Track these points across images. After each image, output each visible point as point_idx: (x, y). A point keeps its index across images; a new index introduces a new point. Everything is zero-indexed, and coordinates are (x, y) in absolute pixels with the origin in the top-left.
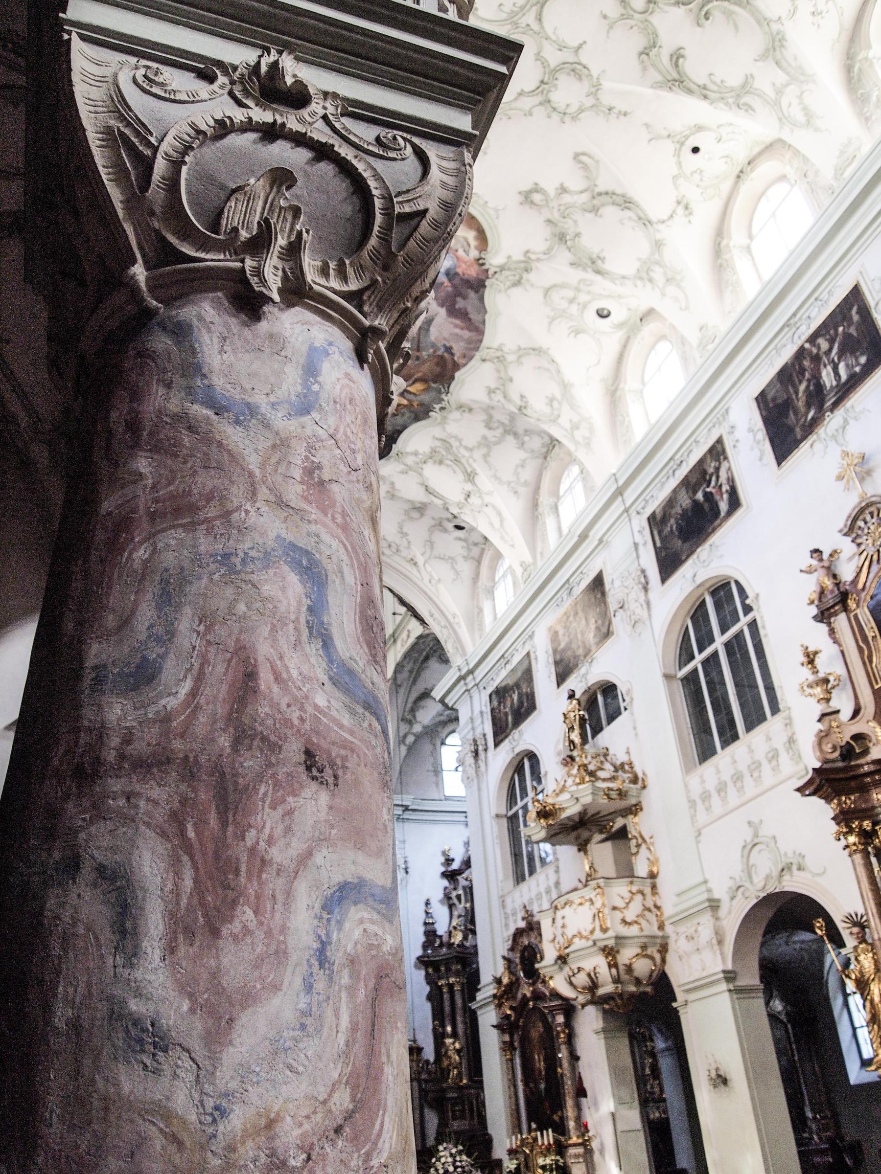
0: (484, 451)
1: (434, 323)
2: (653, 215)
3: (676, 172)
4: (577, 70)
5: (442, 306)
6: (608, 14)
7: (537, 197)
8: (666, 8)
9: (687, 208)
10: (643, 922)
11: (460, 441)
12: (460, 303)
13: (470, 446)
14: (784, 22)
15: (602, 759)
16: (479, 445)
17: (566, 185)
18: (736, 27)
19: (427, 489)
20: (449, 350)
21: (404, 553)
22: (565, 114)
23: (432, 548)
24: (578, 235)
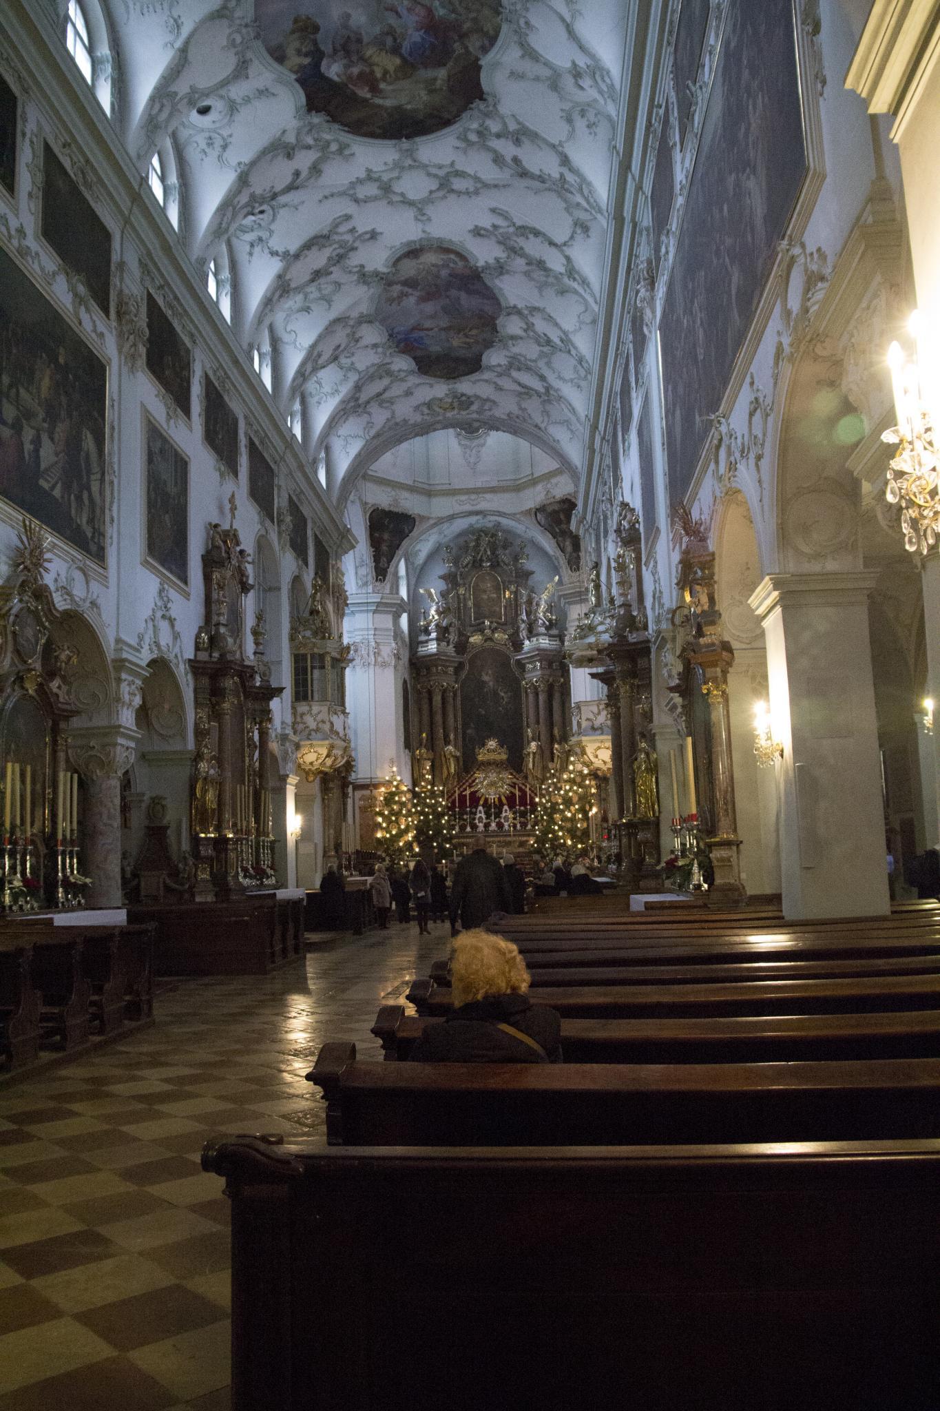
2: (559, 240)
3: (565, 205)
7: (482, 232)
16: (539, 355)
19: (520, 384)
23: (548, 416)
24: (522, 248)
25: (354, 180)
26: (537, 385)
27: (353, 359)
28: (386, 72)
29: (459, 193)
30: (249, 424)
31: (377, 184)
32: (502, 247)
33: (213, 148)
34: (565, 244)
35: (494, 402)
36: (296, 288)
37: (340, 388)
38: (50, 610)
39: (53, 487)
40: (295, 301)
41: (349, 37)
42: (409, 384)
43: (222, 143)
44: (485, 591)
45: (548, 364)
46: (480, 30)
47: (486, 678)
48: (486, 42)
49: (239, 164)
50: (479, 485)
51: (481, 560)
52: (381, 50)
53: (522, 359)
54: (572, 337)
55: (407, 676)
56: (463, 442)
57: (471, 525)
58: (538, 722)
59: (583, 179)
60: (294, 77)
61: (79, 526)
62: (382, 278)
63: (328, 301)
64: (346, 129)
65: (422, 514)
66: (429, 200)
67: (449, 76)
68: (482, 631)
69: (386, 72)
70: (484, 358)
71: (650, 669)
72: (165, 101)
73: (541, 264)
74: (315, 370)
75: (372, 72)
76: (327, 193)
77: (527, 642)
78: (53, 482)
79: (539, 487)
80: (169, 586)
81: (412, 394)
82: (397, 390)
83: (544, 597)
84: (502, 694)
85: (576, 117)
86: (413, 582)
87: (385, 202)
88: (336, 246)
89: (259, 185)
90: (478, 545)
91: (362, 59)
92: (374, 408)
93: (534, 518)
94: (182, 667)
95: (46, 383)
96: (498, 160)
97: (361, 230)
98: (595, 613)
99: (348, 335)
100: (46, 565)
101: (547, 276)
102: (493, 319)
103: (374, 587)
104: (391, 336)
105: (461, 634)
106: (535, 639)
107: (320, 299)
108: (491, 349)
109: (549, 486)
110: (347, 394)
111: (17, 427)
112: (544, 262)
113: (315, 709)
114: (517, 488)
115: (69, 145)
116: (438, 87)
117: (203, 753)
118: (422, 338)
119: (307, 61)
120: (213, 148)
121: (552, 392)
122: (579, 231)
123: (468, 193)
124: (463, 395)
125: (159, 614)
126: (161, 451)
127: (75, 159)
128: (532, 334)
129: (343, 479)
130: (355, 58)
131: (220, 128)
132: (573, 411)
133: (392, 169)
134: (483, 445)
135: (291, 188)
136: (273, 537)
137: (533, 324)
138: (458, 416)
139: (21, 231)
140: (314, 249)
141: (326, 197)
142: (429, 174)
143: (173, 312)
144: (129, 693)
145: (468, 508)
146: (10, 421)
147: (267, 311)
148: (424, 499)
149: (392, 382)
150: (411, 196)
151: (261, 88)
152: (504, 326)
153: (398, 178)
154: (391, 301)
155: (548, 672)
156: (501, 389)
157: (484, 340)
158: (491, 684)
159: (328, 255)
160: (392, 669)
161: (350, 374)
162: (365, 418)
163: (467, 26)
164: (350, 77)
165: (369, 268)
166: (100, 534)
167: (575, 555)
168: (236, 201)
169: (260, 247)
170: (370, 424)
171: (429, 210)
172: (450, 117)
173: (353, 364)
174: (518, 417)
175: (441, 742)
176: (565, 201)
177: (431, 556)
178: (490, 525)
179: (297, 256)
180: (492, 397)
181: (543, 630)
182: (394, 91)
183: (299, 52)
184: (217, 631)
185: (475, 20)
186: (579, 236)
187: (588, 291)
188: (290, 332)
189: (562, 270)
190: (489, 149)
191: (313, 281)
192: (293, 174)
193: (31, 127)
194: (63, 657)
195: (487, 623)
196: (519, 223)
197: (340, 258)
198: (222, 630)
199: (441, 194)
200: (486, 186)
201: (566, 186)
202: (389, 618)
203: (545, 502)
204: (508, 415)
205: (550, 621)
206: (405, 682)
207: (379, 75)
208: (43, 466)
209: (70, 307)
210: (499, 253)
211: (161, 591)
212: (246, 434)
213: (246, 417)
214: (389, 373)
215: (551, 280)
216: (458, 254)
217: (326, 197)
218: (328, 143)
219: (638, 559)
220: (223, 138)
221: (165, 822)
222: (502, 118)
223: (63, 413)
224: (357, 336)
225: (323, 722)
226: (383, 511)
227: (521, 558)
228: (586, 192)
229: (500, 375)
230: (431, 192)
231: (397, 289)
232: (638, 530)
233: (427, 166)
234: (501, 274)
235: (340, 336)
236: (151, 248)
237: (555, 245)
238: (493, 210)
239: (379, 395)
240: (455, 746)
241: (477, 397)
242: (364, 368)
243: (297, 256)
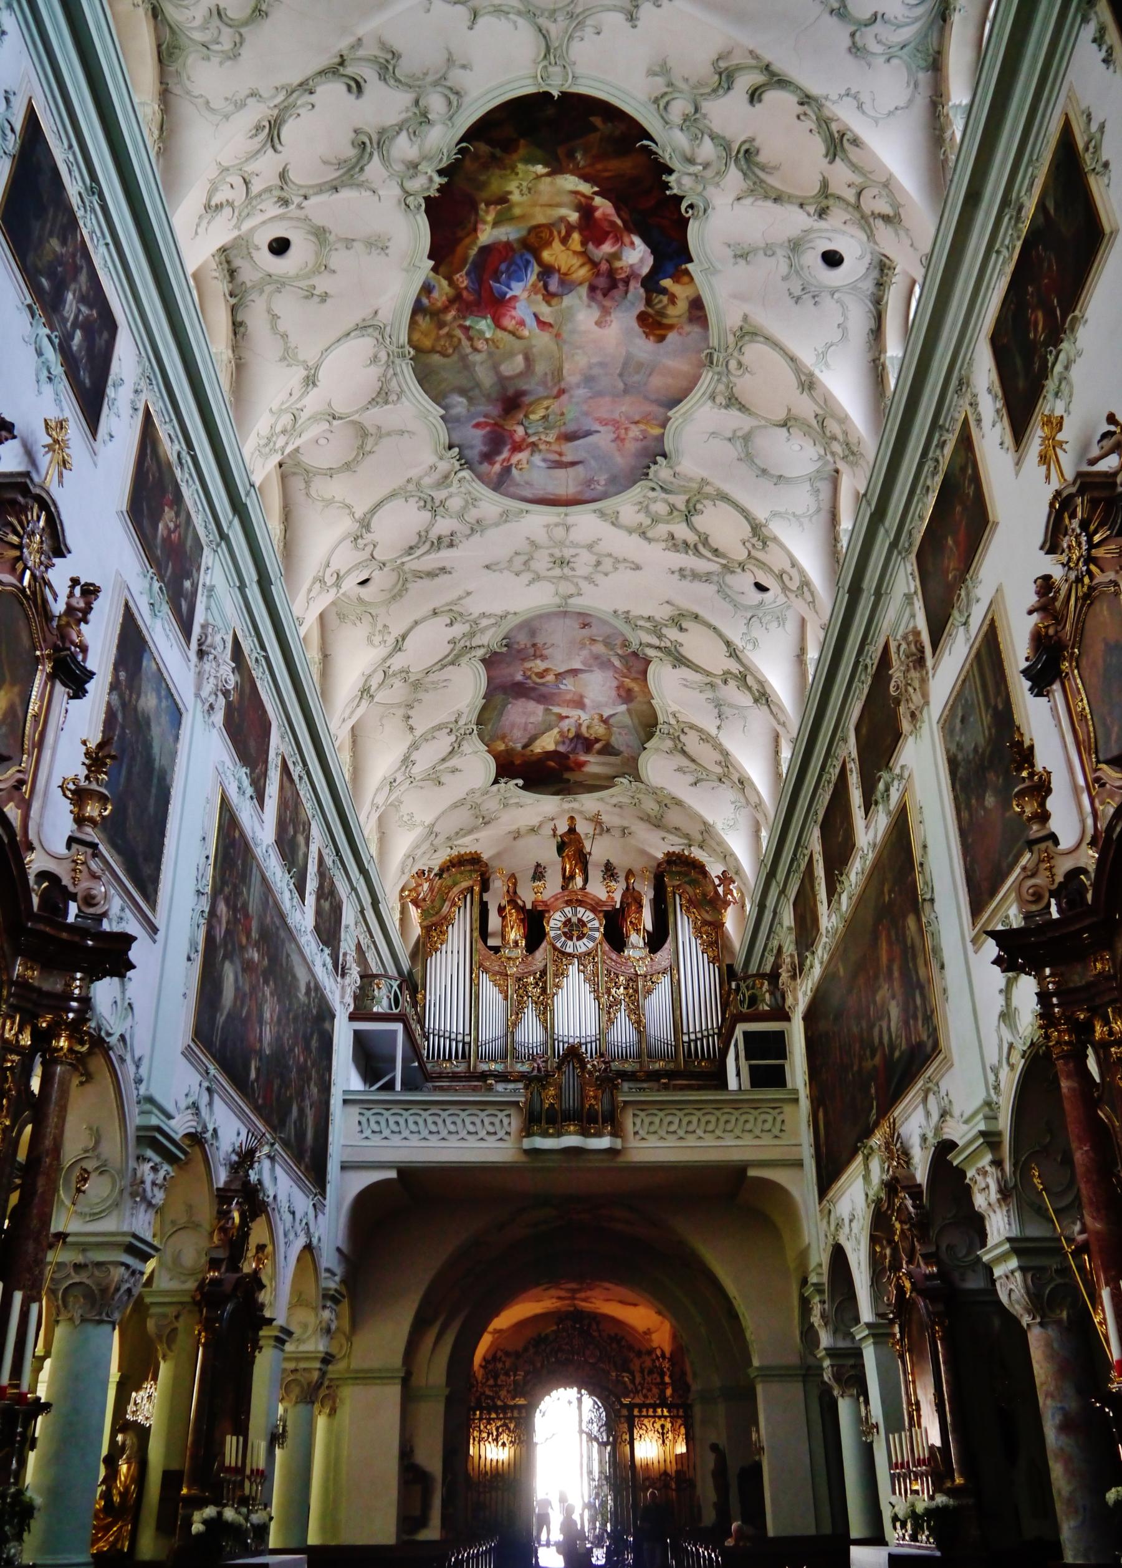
6: (461, 72)
8: (404, 116)
18: (325, 162)
28: (564, 241)
41: (605, 295)
46: (436, 315)
48: (425, 301)
52: (566, 274)
60: (690, 266)
67: (475, 230)
69: (564, 241)
75: (584, 243)
91: (594, 264)
116: (492, 207)
119: (666, 283)
130: (604, 267)
151: (742, 262)
163: (450, 316)
164: (618, 239)
182: (558, 205)
183: (673, 299)
185: (441, 325)
207: (576, 236)
233: (519, 13)
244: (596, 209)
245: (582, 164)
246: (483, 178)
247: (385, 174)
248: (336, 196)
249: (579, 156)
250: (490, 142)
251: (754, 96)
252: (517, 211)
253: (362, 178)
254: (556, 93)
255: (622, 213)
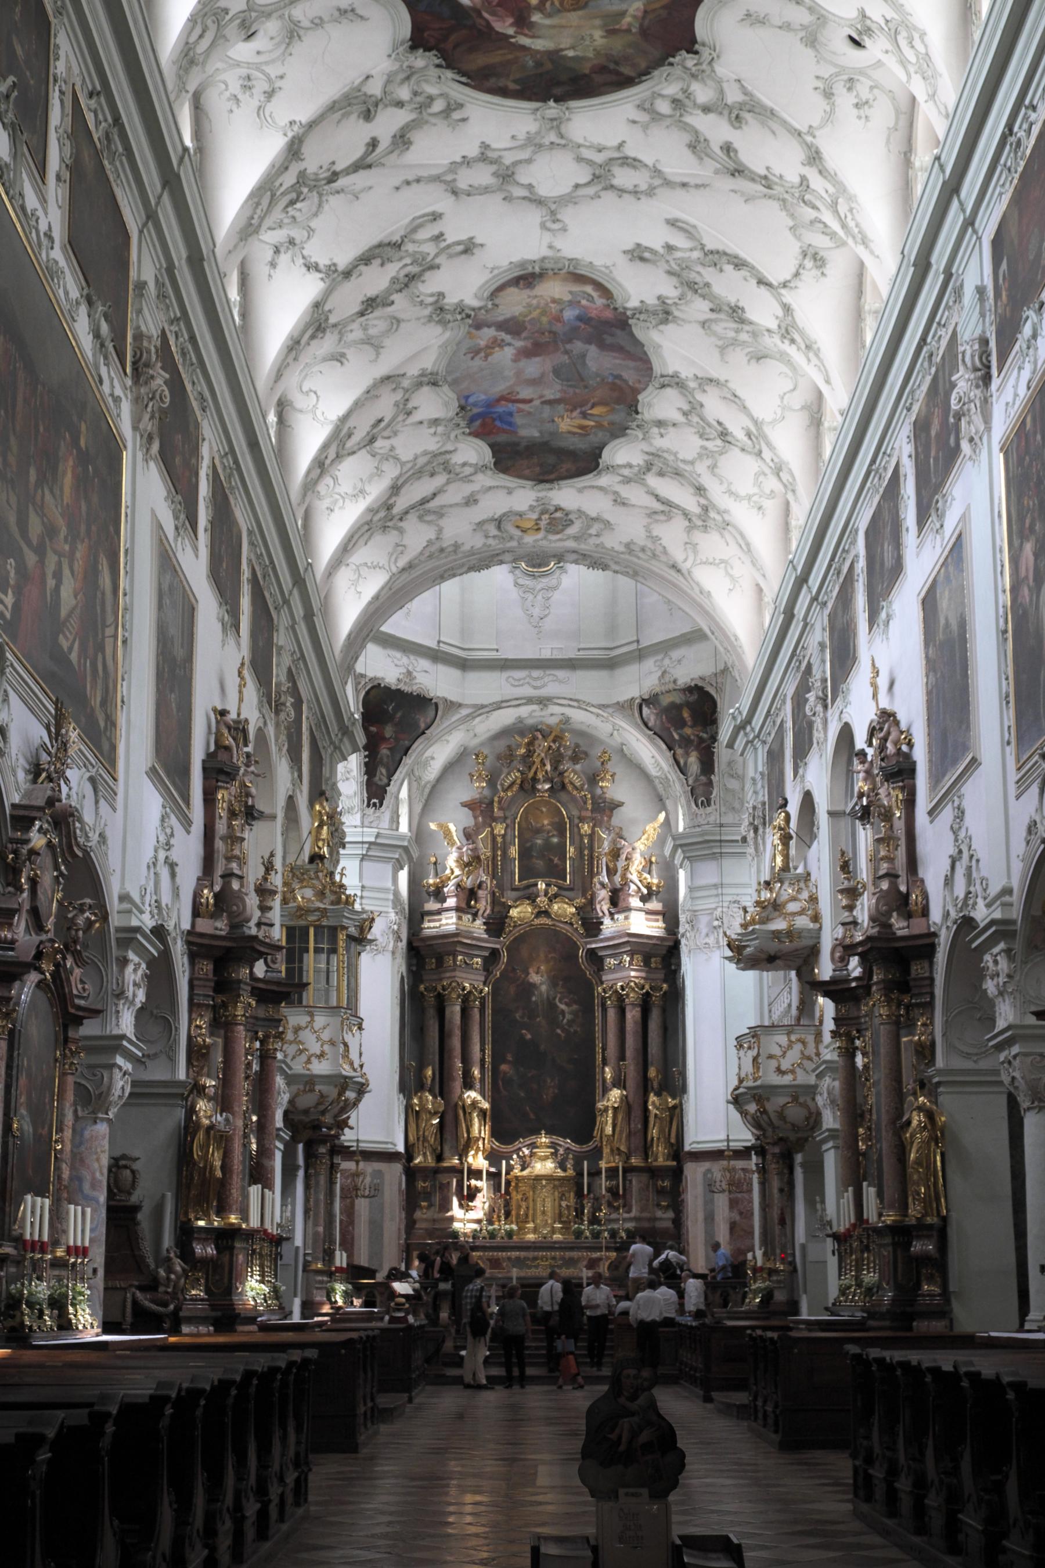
0: (709, 462)
1: (588, 358)
3: (791, 223)
4: (630, 163)
5: (590, 343)
7: (647, 255)
9: (815, 257)
10: (798, 1070)
11: (675, 454)
12: (609, 340)
13: (690, 458)
14: (817, 133)
15: (802, 885)
16: (700, 456)
17: (672, 242)
19: (657, 498)
20: (619, 377)
21: (663, 558)
22: (636, 192)
23: (695, 552)
24: (707, 285)
25: (458, 159)
26: (689, 502)
27: (394, 441)
29: (621, 191)
30: (251, 544)
31: (494, 168)
32: (674, 281)
33: (252, 96)
34: (785, 285)
35: (607, 524)
36: (335, 326)
37: (368, 489)
38: (70, 847)
39: (71, 648)
40: (327, 344)
42: (475, 487)
43: (266, 87)
44: (538, 831)
45: (713, 468)
47: (535, 978)
49: (292, 123)
50: (546, 654)
51: (535, 780)
53: (671, 458)
54: (767, 429)
55: (403, 969)
56: (520, 581)
57: (520, 720)
58: (622, 1057)
59: (841, 188)
61: (93, 710)
62: (468, 316)
63: (375, 345)
64: (464, 79)
65: (453, 697)
66: (569, 199)
67: (645, 12)
68: (532, 898)
70: (605, 453)
71: (932, 980)
72: (209, 22)
73: (736, 313)
74: (339, 457)
76: (410, 178)
77: (607, 921)
78: (71, 637)
79: (649, 664)
80: (173, 811)
81: (476, 501)
82: (455, 493)
83: (640, 846)
84: (563, 1007)
85: (839, 89)
86: (418, 808)
87: (498, 197)
88: (408, 261)
89: (313, 161)
90: (530, 753)
92: (411, 524)
93: (637, 714)
94: (179, 942)
95: (68, 480)
96: (697, 145)
97: (450, 238)
98: (782, 882)
99: (396, 404)
100: (69, 773)
101: (737, 331)
102: (636, 392)
103: (363, 816)
104: (462, 408)
105: (495, 901)
106: (620, 917)
107: (363, 342)
108: (622, 440)
109: (667, 662)
110: (375, 501)
111: (40, 551)
112: (743, 309)
113: (320, 1021)
114: (610, 664)
115: (98, 94)
116: (624, 27)
117: (204, 1087)
118: (511, 414)
120: (252, 96)
121: (712, 514)
122: (809, 263)
123: (635, 193)
124: (558, 509)
125: (162, 855)
126: (171, 588)
127: (101, 117)
128: (695, 419)
129: (349, 635)
131: (266, 63)
132: (747, 548)
133: (522, 147)
134: (555, 588)
135: (360, 165)
136: (271, 730)
137: (702, 406)
138: (544, 543)
139: (49, 236)
140: (377, 262)
141: (408, 183)
142: (579, 159)
143: (184, 360)
144: (135, 984)
145: (527, 691)
146: (35, 543)
147: (290, 360)
148: (455, 673)
149: (448, 482)
150: (544, 190)
152: (650, 405)
153: (529, 161)
154: (475, 352)
155: (643, 974)
156: (624, 504)
157: (611, 423)
158: (544, 988)
159: (393, 274)
160: (389, 955)
161: (386, 466)
162: (393, 537)
165: (451, 300)
166: (112, 723)
167: (703, 778)
168: (277, 184)
169: (290, 253)
170: (400, 548)
171: (567, 215)
172: (633, 74)
173: (392, 448)
174: (643, 550)
175: (458, 1084)
176: (792, 216)
177: (449, 769)
178: (553, 721)
179: (347, 274)
180: (606, 516)
181: (635, 902)
182: (553, 27)
184: (226, 886)
186: (809, 274)
187: (814, 360)
188: (307, 393)
189: (773, 325)
190: (686, 127)
191: (362, 314)
192: (368, 145)
193: (60, 67)
194: (80, 921)
195: (541, 886)
196: (709, 246)
197: (411, 278)
198: (235, 885)
199: (591, 191)
200: (668, 183)
201: (807, 197)
202: (389, 868)
203: (658, 690)
204: (628, 545)
205: (648, 887)
206: (402, 977)
208: (63, 613)
209: (90, 354)
210: (669, 289)
211: (163, 820)
212: (250, 561)
213: (250, 533)
214: (447, 468)
215: (744, 337)
216: (599, 286)
217: (408, 183)
218: (431, 99)
219: (910, 803)
220: (270, 80)
221: (134, 1199)
222: (719, 82)
223: (83, 528)
224: (410, 405)
225: (332, 1043)
226: (388, 689)
227: (602, 780)
228: (843, 209)
229: (627, 481)
230: (577, 186)
231: (489, 333)
232: (908, 757)
233: (579, 146)
234: (665, 321)
235: (385, 406)
236: (177, 264)
237: (769, 285)
238: (673, 223)
239: (424, 501)
240: (482, 1094)
241: (580, 512)
242: (411, 457)
243: (347, 274)
244: (512, 25)
245: (528, 58)
246: (630, 51)
247: (725, 85)
248: (776, 108)
249: (531, 63)
250: (618, 73)
251: (374, 143)
252: (598, 22)
253: (747, 98)
254: (551, 103)
255: (483, 23)
